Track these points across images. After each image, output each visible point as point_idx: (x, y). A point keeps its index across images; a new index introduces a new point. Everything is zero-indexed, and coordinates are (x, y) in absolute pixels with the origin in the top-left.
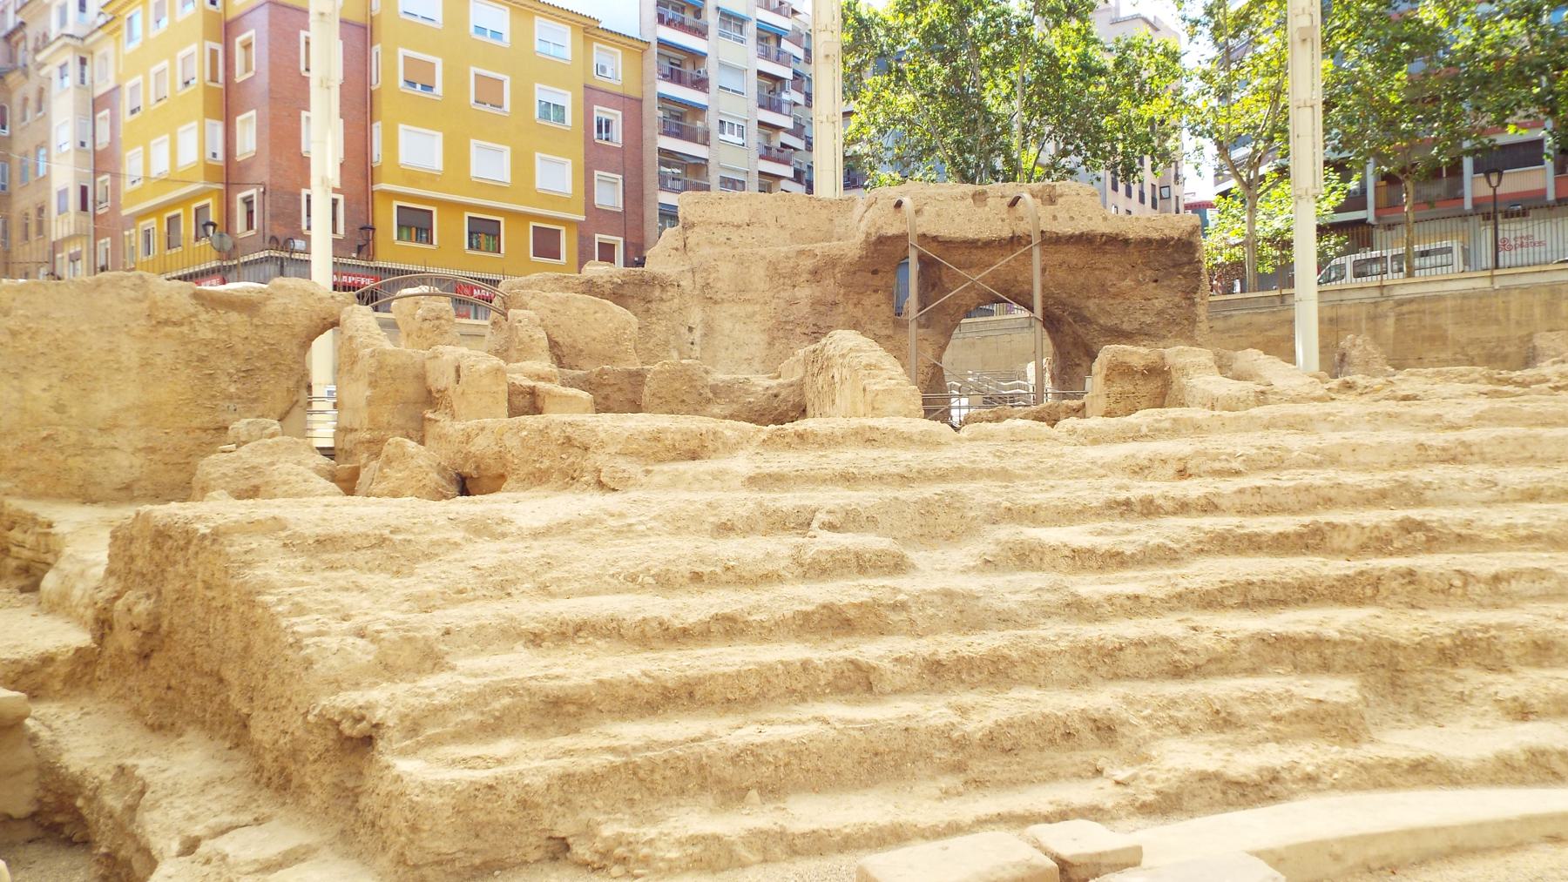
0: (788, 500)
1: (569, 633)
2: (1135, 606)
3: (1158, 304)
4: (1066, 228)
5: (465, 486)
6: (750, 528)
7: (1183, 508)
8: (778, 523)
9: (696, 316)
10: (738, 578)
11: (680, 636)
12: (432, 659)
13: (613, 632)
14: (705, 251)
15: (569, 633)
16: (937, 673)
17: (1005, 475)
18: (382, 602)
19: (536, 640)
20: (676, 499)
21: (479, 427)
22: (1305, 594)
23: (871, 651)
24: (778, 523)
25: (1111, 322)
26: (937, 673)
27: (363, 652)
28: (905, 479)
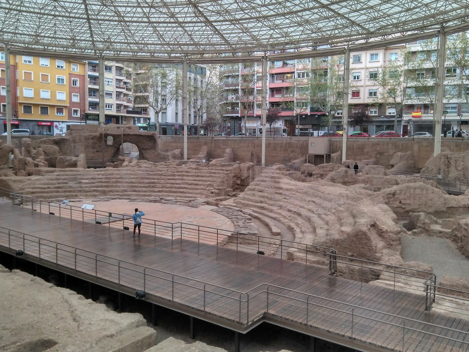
0: (59, 177)
1: (35, 188)
2: (87, 187)
3: (150, 144)
4: (132, 133)
5: (29, 175)
6: (55, 180)
7: (99, 179)
8: (57, 179)
9: (72, 145)
10: (51, 184)
11: (45, 188)
12: (23, 189)
13: (39, 188)
14: (75, 134)
15: (35, 188)
16: (65, 191)
17: (83, 175)
18: (20, 185)
19: (32, 188)
20: (50, 177)
21: (31, 168)
22: (102, 187)
23: (60, 190)
24: (57, 179)
25: (143, 147)
26: (65, 191)
27: (18, 189)
28: (73, 175)
